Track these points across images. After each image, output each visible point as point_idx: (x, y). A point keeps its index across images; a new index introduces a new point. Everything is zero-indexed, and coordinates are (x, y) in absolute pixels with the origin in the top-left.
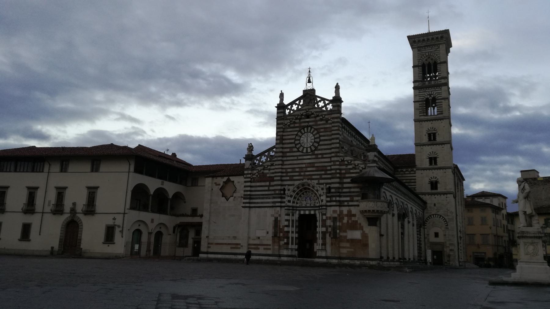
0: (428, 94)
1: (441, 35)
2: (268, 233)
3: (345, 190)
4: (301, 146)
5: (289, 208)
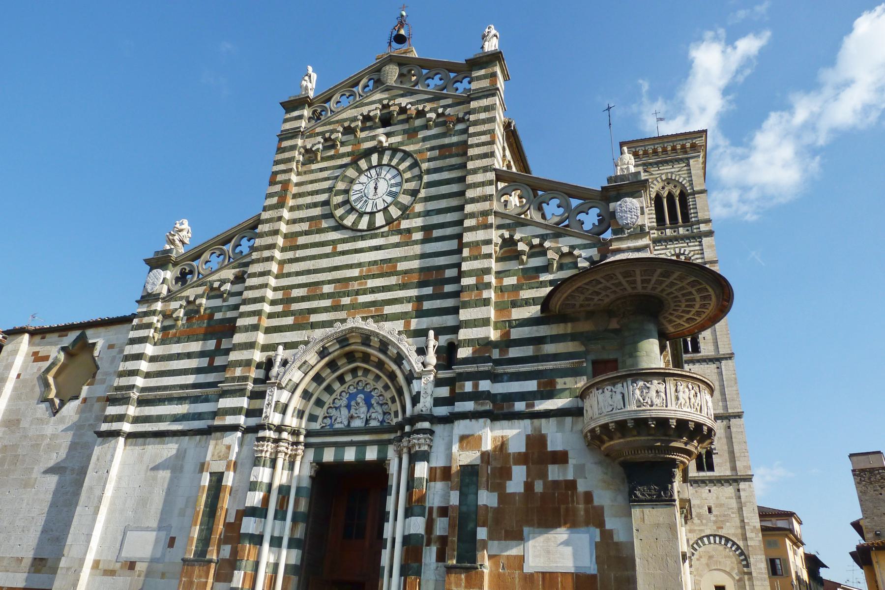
0: (673, 253)
2: (172, 542)
3: (514, 352)
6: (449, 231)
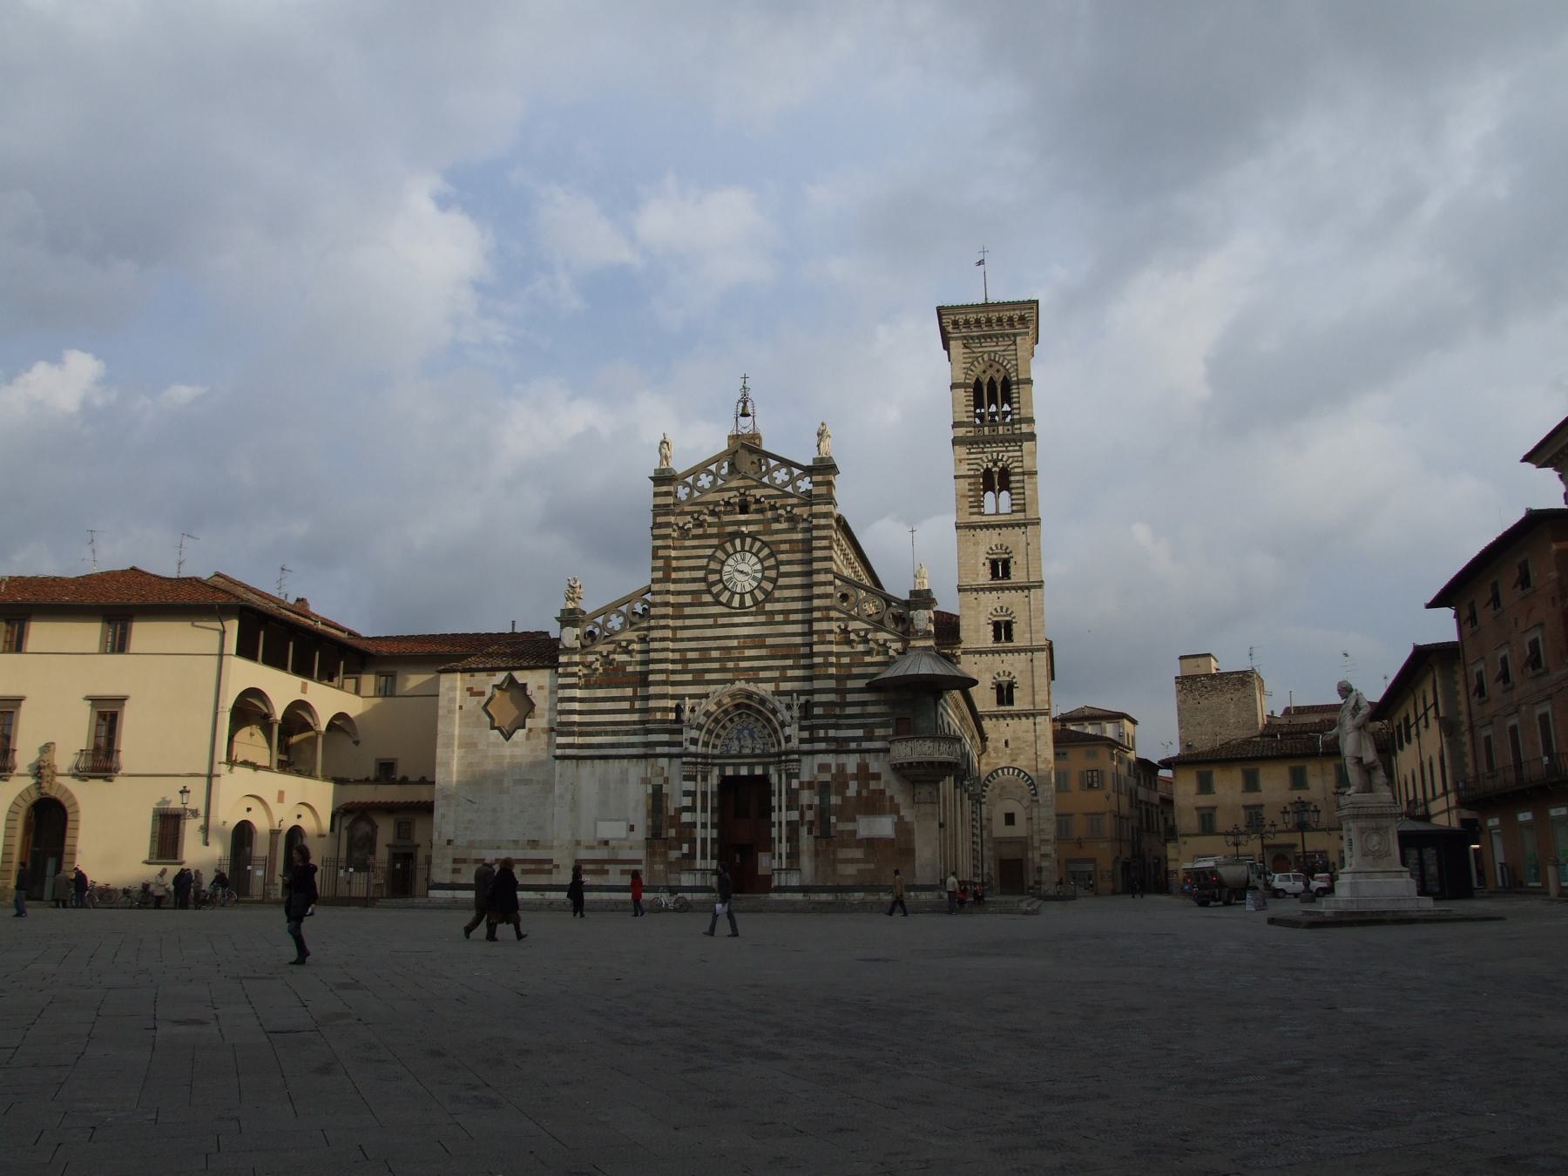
0: (990, 458)
1: (1018, 312)
2: (632, 828)
3: (849, 711)
4: (726, 588)
5: (694, 760)
6: (799, 617)
